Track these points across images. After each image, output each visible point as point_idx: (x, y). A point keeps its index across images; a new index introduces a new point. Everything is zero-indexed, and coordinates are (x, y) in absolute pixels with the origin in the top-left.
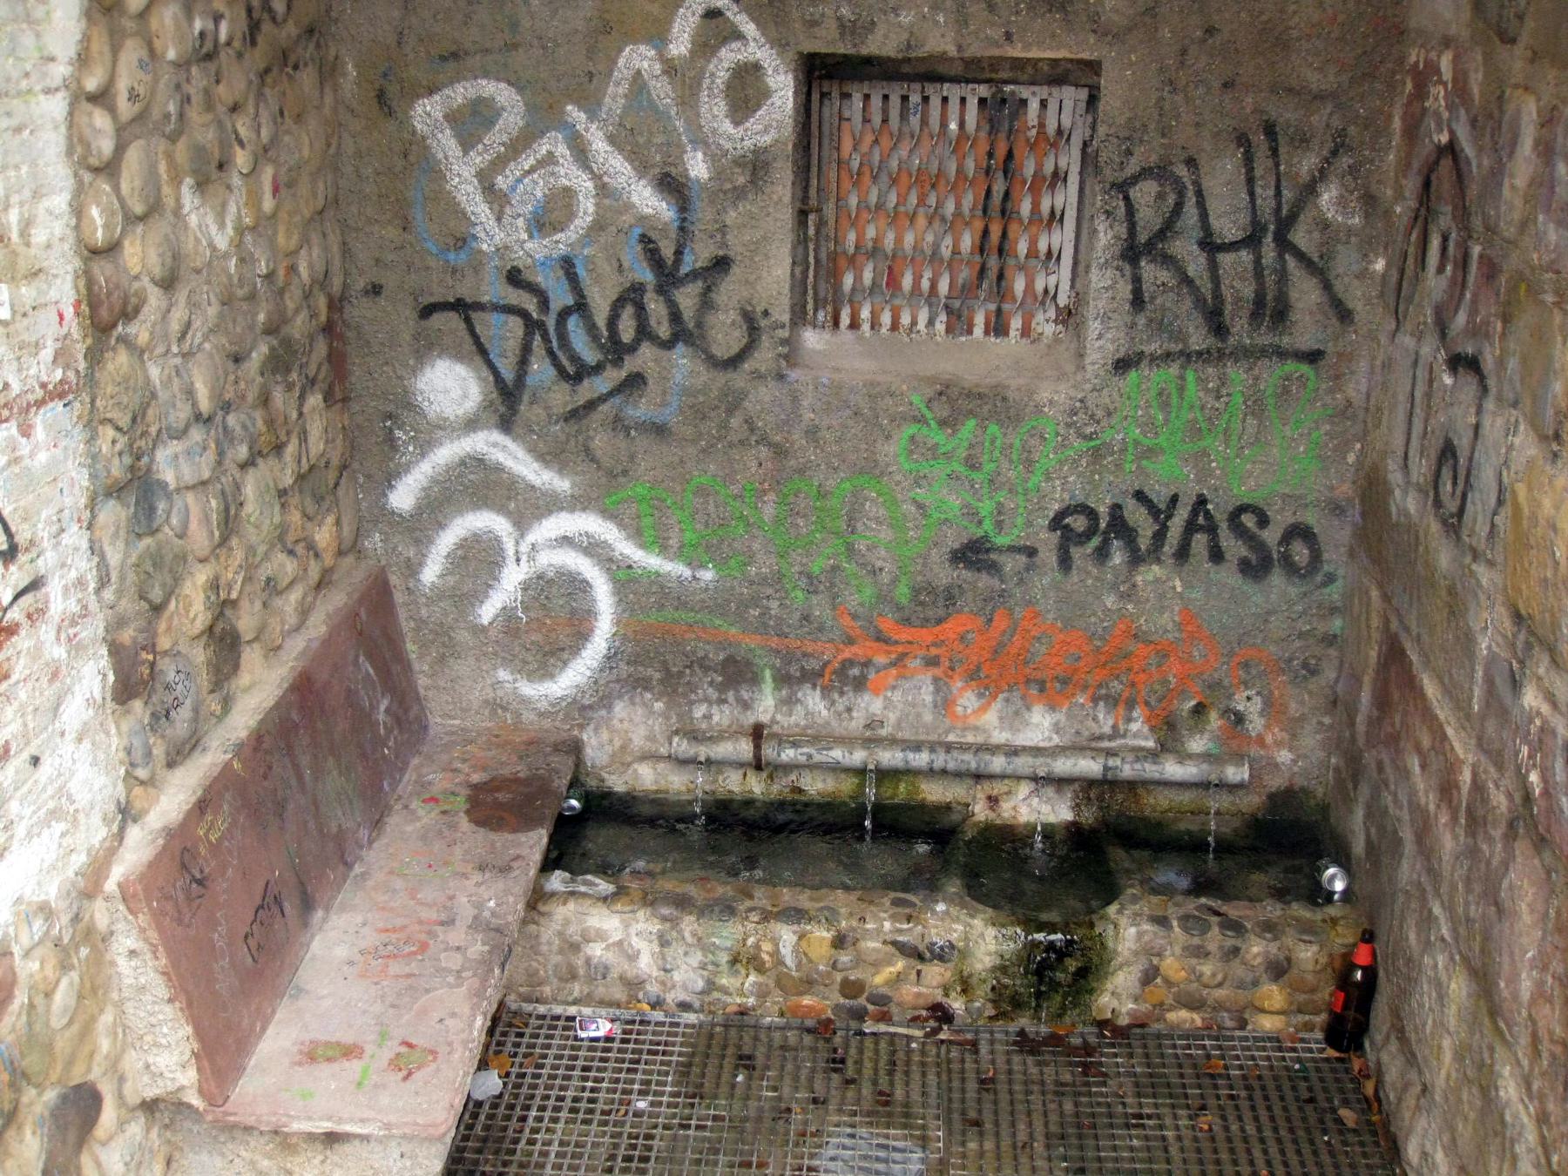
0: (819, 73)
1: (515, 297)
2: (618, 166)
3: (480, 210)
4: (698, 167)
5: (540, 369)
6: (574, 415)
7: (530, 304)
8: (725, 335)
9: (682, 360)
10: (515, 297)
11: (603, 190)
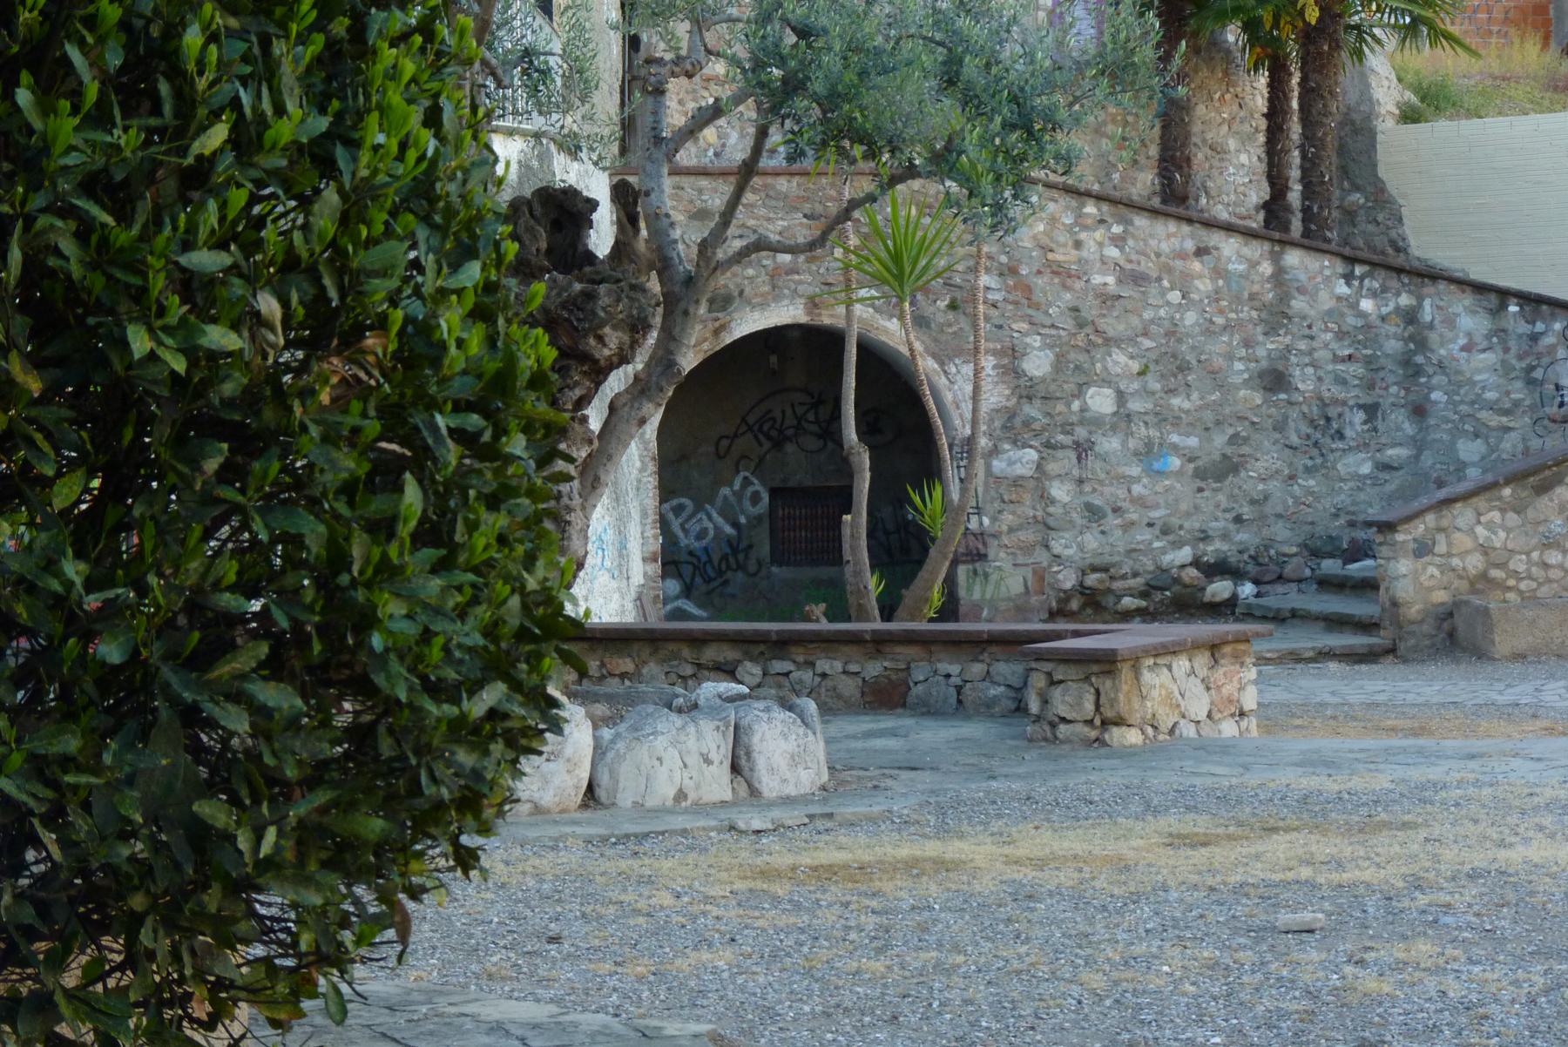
0: (774, 492)
1: (690, 559)
2: (720, 520)
3: (681, 534)
4: (743, 520)
5: (698, 580)
6: (709, 593)
7: (695, 561)
8: (752, 568)
9: (740, 575)
10: (690, 559)
11: (716, 528)
